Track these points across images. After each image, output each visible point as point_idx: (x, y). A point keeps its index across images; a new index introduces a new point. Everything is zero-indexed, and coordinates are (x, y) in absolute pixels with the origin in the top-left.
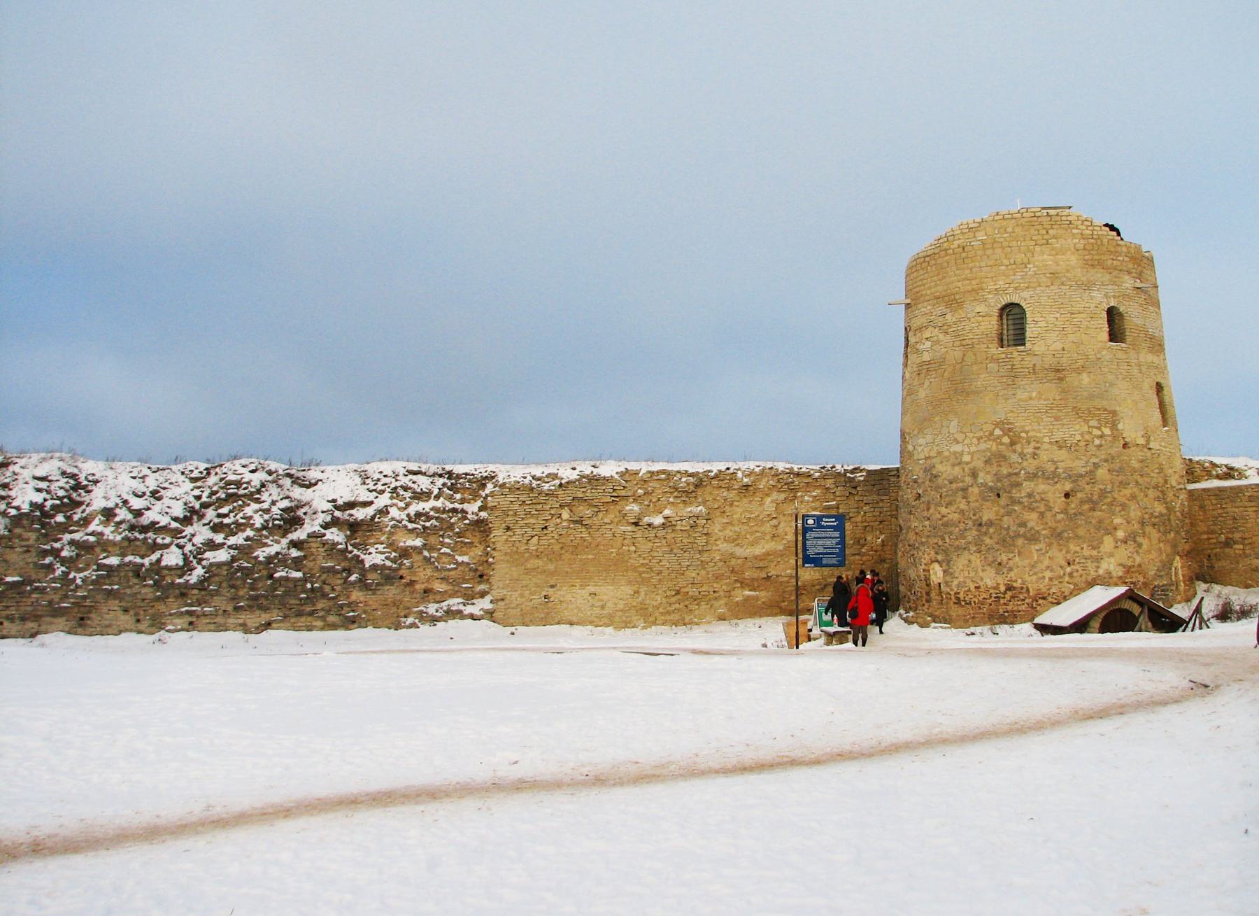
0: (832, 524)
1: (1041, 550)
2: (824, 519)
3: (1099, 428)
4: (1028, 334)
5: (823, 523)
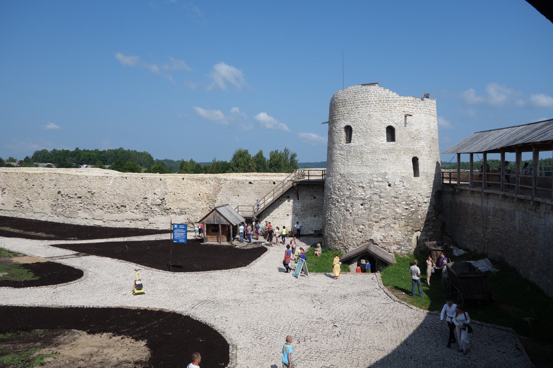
0: (183, 227)
1: (350, 226)
2: (180, 226)
3: (377, 178)
4: (353, 138)
5: (180, 227)
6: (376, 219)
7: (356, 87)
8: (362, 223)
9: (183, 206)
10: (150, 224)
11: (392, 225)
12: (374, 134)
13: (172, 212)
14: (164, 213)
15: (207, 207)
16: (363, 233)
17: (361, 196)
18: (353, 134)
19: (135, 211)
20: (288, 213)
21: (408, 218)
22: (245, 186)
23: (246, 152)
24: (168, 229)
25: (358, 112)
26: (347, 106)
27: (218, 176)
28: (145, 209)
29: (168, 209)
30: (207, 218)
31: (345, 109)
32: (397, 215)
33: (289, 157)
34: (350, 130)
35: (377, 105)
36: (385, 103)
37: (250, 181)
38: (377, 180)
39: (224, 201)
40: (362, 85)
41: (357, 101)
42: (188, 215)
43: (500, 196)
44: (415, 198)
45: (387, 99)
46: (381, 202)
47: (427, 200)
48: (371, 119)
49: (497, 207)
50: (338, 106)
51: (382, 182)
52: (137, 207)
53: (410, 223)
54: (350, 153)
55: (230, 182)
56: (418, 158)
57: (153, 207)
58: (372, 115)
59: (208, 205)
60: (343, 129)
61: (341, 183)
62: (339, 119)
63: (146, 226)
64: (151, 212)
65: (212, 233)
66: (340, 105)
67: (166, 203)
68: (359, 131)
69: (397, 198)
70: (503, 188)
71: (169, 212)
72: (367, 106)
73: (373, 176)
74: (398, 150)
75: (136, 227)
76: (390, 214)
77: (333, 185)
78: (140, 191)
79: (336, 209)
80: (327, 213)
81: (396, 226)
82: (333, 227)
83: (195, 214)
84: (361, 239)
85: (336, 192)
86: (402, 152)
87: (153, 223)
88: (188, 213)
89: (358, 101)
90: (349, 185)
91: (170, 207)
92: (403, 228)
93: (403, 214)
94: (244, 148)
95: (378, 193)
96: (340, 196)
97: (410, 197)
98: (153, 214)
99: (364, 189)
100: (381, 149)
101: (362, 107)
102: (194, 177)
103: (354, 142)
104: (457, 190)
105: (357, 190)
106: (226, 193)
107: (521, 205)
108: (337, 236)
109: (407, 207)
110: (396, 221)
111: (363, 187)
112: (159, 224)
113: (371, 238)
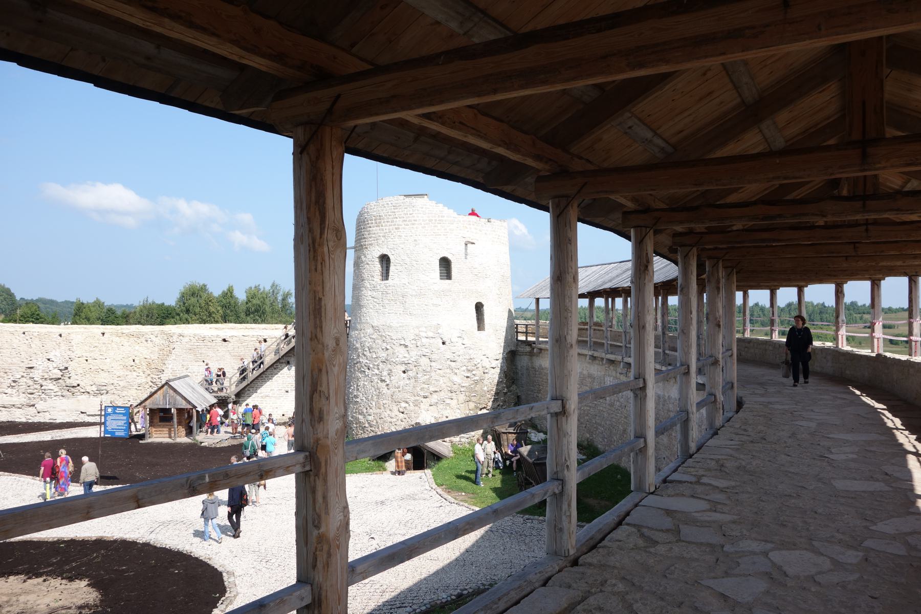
0: (122, 412)
1: (386, 404)
2: (118, 409)
3: (426, 332)
4: (391, 273)
5: (117, 411)
6: (424, 393)
7: (396, 199)
8: (404, 399)
9: (103, 380)
10: (39, 412)
11: (448, 401)
12: (422, 268)
13: (83, 391)
14: (65, 393)
15: (148, 381)
16: (406, 414)
17: (403, 360)
18: (392, 268)
19: (9, 391)
20: (287, 389)
21: (470, 389)
22: (216, 345)
23: (204, 288)
24: (73, 421)
25: (398, 234)
26: (382, 226)
27: (167, 330)
28: (29, 386)
29: (73, 387)
30: (151, 399)
31: (380, 230)
32: (455, 386)
33: (280, 298)
34: (387, 261)
35: (426, 226)
36: (438, 223)
37: (224, 338)
38: (426, 336)
39: (178, 371)
40: (405, 196)
41: (398, 220)
42: (113, 396)
43: (588, 356)
44: (479, 361)
45: (440, 218)
46: (432, 368)
47: (498, 364)
48: (417, 246)
49: (585, 372)
50: (370, 225)
51: (432, 338)
52: (13, 384)
53: (472, 398)
54: (387, 295)
55: (190, 339)
56: (483, 303)
57: (44, 383)
58: (419, 240)
59: (149, 379)
60: (377, 260)
61: (373, 340)
62: (371, 244)
63: (31, 418)
64: (41, 391)
65: (160, 424)
66: (372, 223)
67: (70, 375)
68: (401, 262)
69: (454, 361)
70: (590, 346)
71: (77, 391)
72: (413, 227)
73: (420, 329)
74: (455, 293)
75: (10, 420)
76: (444, 386)
78: (19, 356)
79: (365, 379)
80: (351, 386)
81: (453, 403)
82: (360, 406)
83: (124, 393)
84: (403, 423)
85: (365, 353)
86: (461, 294)
87: (44, 412)
88: (112, 392)
89: (399, 219)
90: (385, 344)
91: (78, 382)
92: (462, 405)
93: (463, 385)
94: (199, 281)
95: (427, 354)
96: (371, 360)
97: (472, 360)
98: (45, 396)
99: (408, 349)
100: (432, 289)
101: (404, 228)
102: (124, 332)
103: (392, 280)
104: (535, 349)
105: (396, 351)
106: (181, 357)
107: (611, 368)
108: (367, 420)
109: (468, 375)
110: (454, 394)
111: (406, 346)
112: (55, 412)
113: (418, 421)
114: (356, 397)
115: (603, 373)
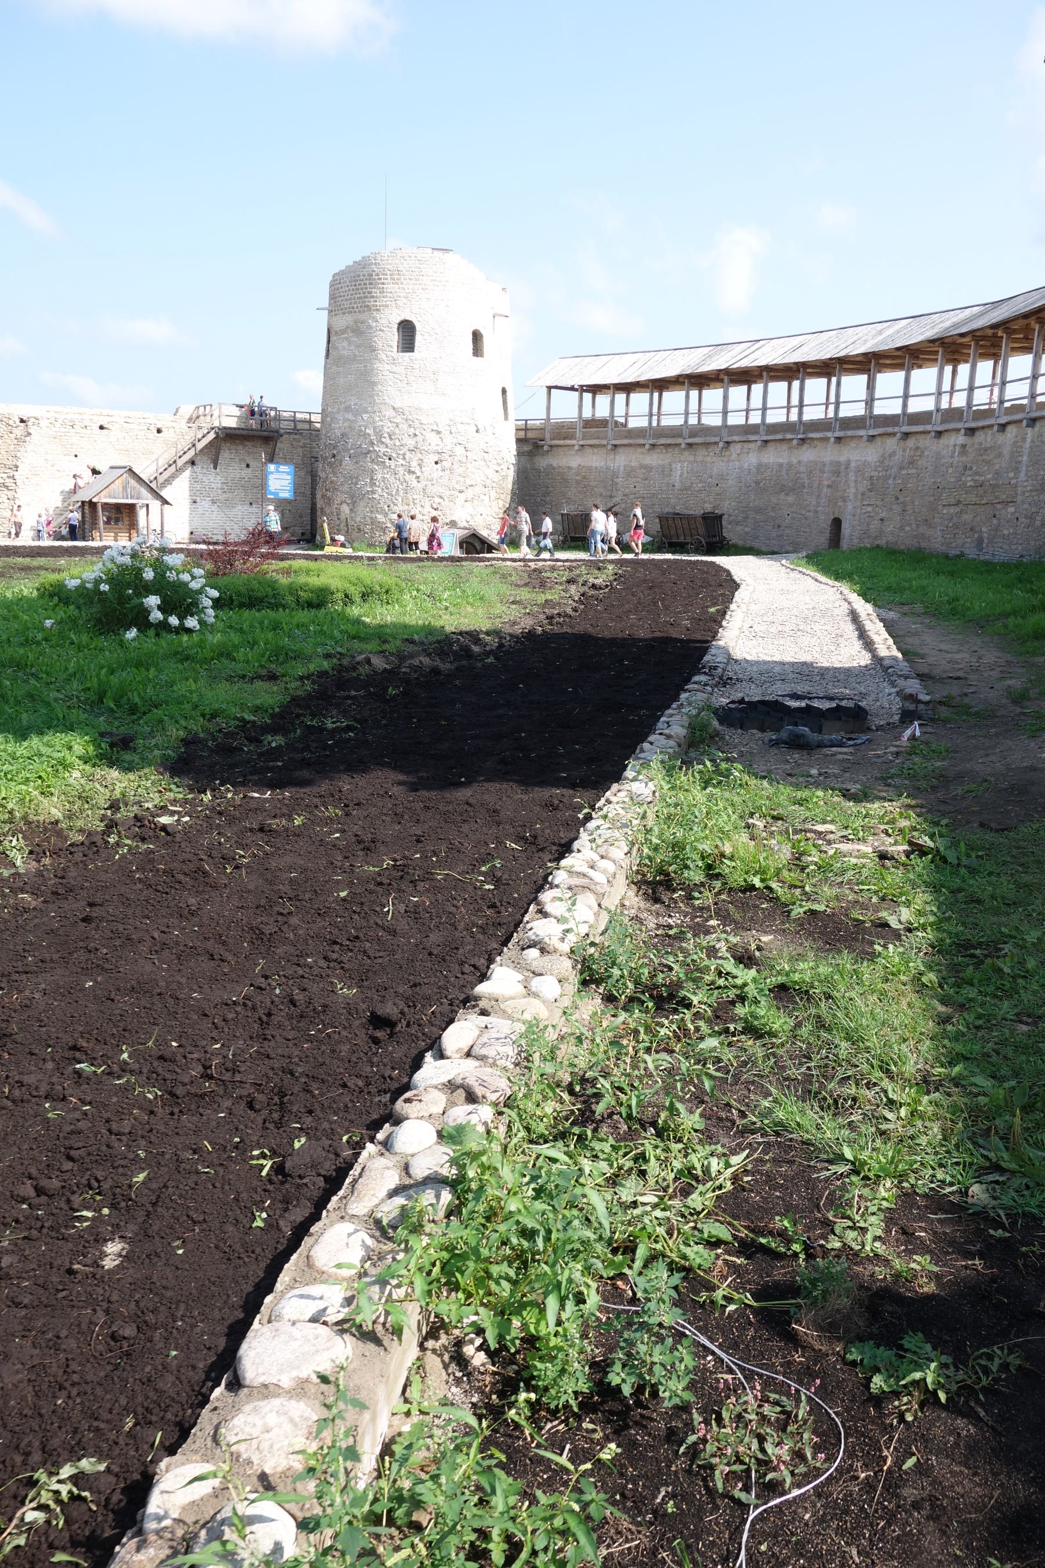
4: (417, 344)
18: (418, 338)
62: (386, 306)
77: (375, 428)
111: (439, 433)
114: (373, 492)
115: (667, 461)
